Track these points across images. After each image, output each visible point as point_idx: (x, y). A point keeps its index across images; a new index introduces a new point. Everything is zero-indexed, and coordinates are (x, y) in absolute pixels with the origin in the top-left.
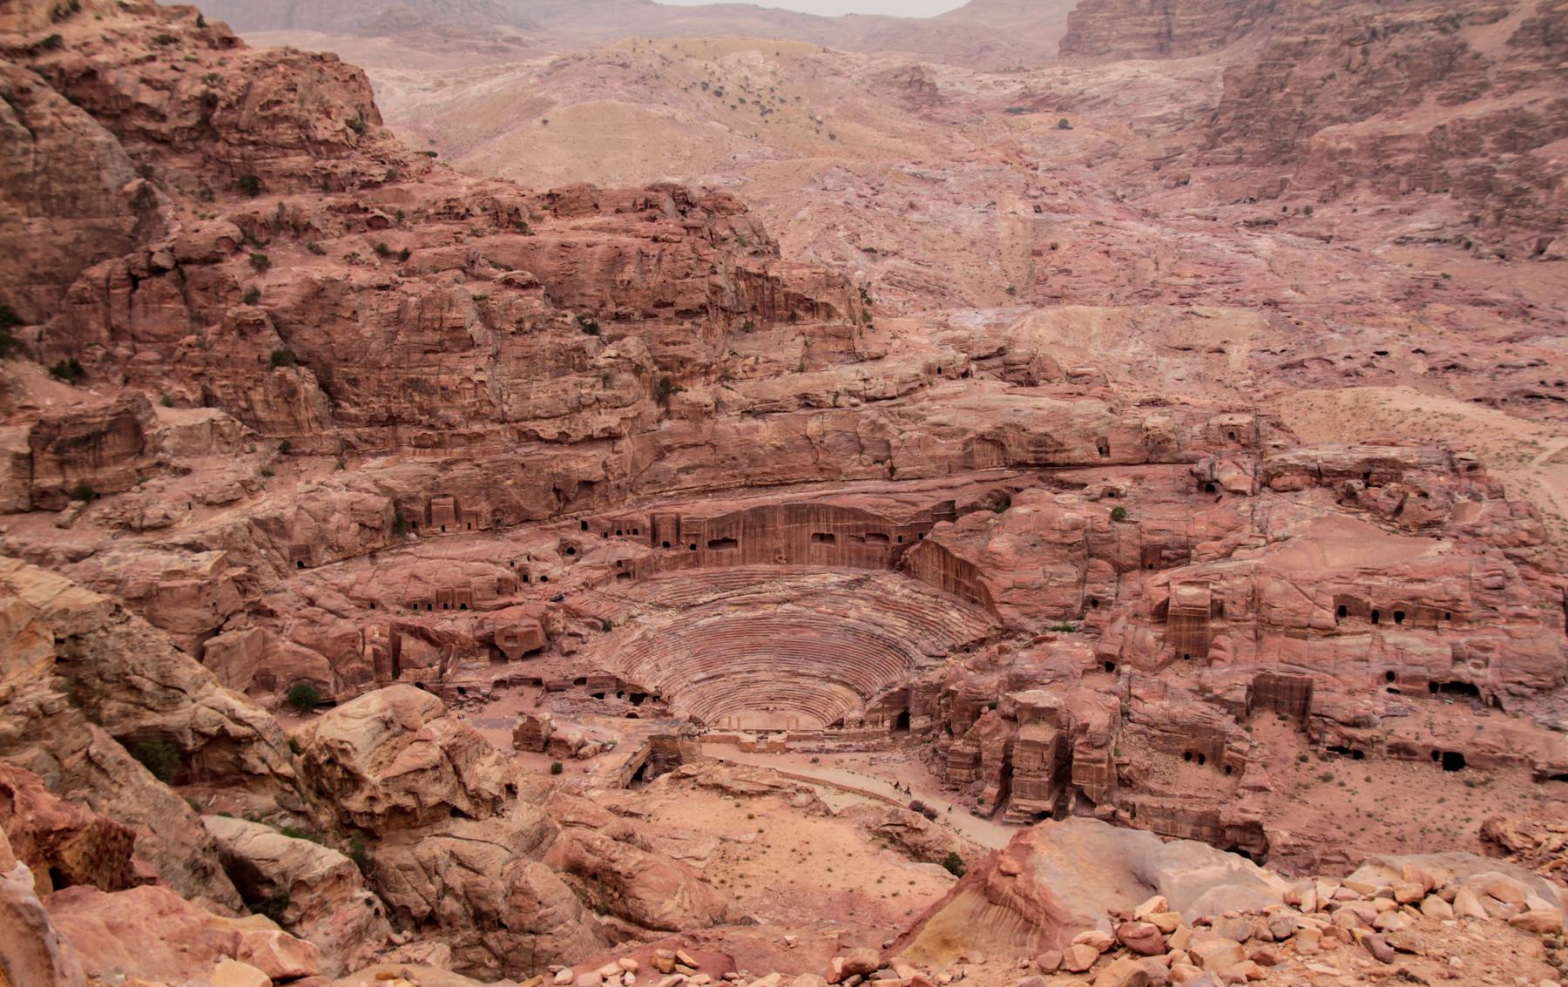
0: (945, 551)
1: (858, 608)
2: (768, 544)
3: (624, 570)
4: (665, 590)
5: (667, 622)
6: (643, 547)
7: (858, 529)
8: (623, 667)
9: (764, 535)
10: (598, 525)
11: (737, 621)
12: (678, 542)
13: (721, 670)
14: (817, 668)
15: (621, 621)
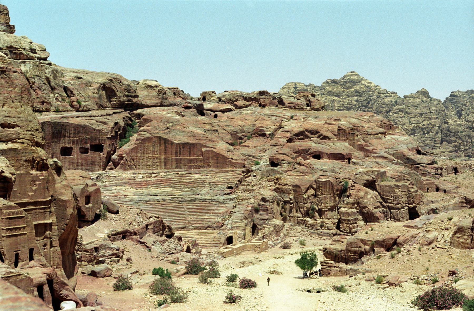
0: (166, 141)
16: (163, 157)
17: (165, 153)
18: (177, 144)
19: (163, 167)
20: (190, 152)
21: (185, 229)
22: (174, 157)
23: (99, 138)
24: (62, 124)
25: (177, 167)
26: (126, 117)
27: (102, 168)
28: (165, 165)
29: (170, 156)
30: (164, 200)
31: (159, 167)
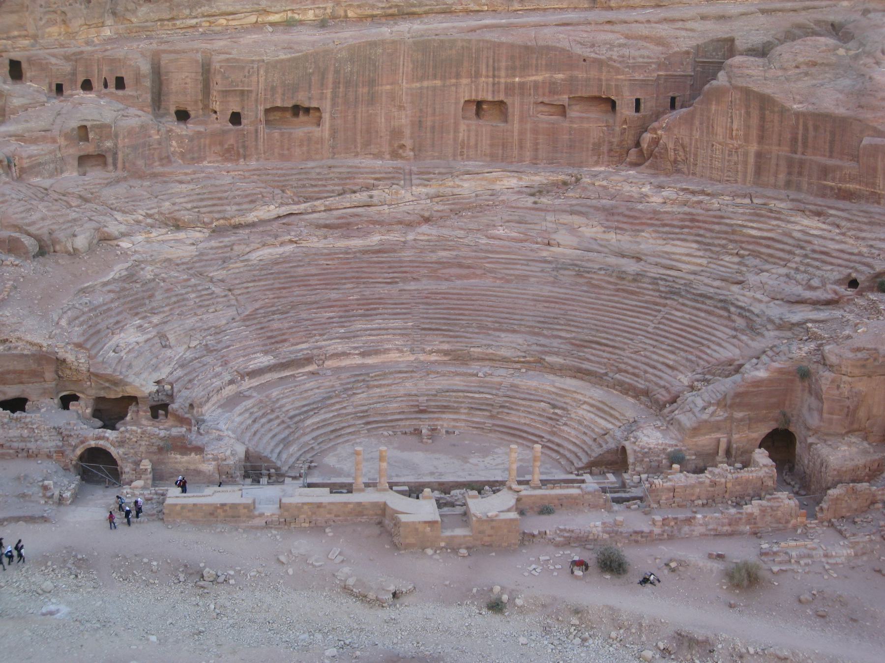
0: (765, 102)
1: (573, 230)
2: (381, 121)
3: (93, 151)
4: (179, 195)
5: (186, 252)
6: (132, 111)
7: (553, 88)
8: (77, 333)
9: (372, 100)
10: (43, 67)
11: (331, 254)
12: (208, 110)
13: (304, 348)
14: (509, 344)
15: (81, 242)
16: (753, 148)
17: (761, 139)
18: (798, 115)
19: (750, 177)
20: (832, 142)
21: (593, 379)
22: (785, 151)
23: (600, 80)
24: (460, 44)
25: (788, 184)
26: (818, 22)
27: (606, 158)
28: (759, 171)
29: (775, 148)
30: (637, 277)
31: (740, 175)
